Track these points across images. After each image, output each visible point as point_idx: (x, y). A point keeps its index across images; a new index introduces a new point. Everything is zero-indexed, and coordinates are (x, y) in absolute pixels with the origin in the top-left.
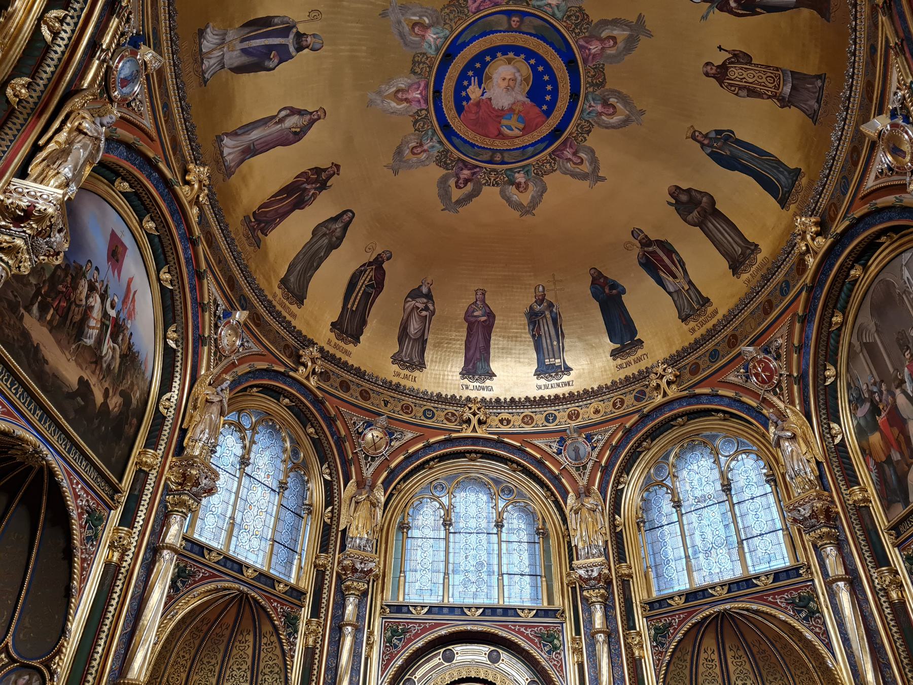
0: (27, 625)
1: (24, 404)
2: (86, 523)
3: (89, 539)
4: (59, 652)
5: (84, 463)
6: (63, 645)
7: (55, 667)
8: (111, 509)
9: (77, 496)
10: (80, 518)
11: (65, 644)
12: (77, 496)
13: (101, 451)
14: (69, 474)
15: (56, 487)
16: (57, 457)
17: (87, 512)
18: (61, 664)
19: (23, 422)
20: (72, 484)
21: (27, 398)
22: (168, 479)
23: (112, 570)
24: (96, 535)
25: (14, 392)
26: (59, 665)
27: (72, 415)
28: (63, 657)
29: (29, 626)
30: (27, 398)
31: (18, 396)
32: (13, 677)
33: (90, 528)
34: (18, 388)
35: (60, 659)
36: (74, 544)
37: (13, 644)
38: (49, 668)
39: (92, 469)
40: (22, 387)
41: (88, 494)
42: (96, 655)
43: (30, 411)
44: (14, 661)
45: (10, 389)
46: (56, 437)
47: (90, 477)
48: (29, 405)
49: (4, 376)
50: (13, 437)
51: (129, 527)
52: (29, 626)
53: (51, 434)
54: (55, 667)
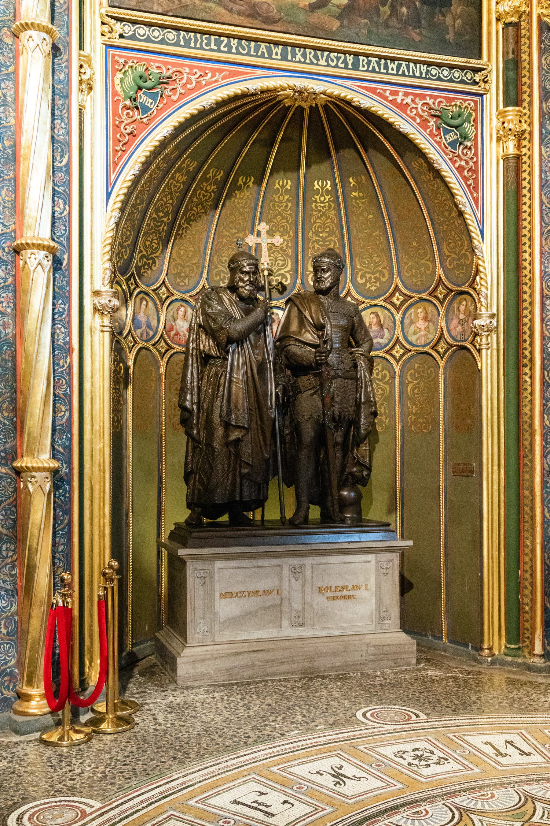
0: (447, 253)
1: (248, 54)
2: (438, 128)
3: (452, 144)
4: (477, 272)
5: (391, 65)
6: (477, 265)
7: (479, 287)
8: (481, 95)
9: (403, 107)
10: (425, 128)
11: (480, 262)
12: (403, 107)
13: (417, 38)
14: (373, 90)
15: (367, 114)
16: (339, 81)
17: (434, 116)
18: (483, 283)
19: (260, 72)
20: (386, 98)
21: (248, 46)
22: (539, 17)
23: (512, 163)
24: (466, 138)
25: (226, 49)
26: (481, 285)
27: (335, 24)
28: (482, 276)
29: (449, 254)
30: (248, 46)
31: (234, 50)
32: (455, 305)
33: (446, 132)
34: (229, 43)
35: (481, 278)
36: (431, 158)
37: (445, 275)
38: (475, 289)
39: (412, 65)
40: (234, 38)
41: (423, 97)
42: (524, 263)
43: (262, 56)
44: (452, 291)
45: (219, 50)
46: (323, 62)
47: (414, 76)
48: (256, 51)
49: (202, 41)
50: (253, 95)
51: (517, 105)
52: (449, 254)
53: (312, 63)
54: (479, 287)
